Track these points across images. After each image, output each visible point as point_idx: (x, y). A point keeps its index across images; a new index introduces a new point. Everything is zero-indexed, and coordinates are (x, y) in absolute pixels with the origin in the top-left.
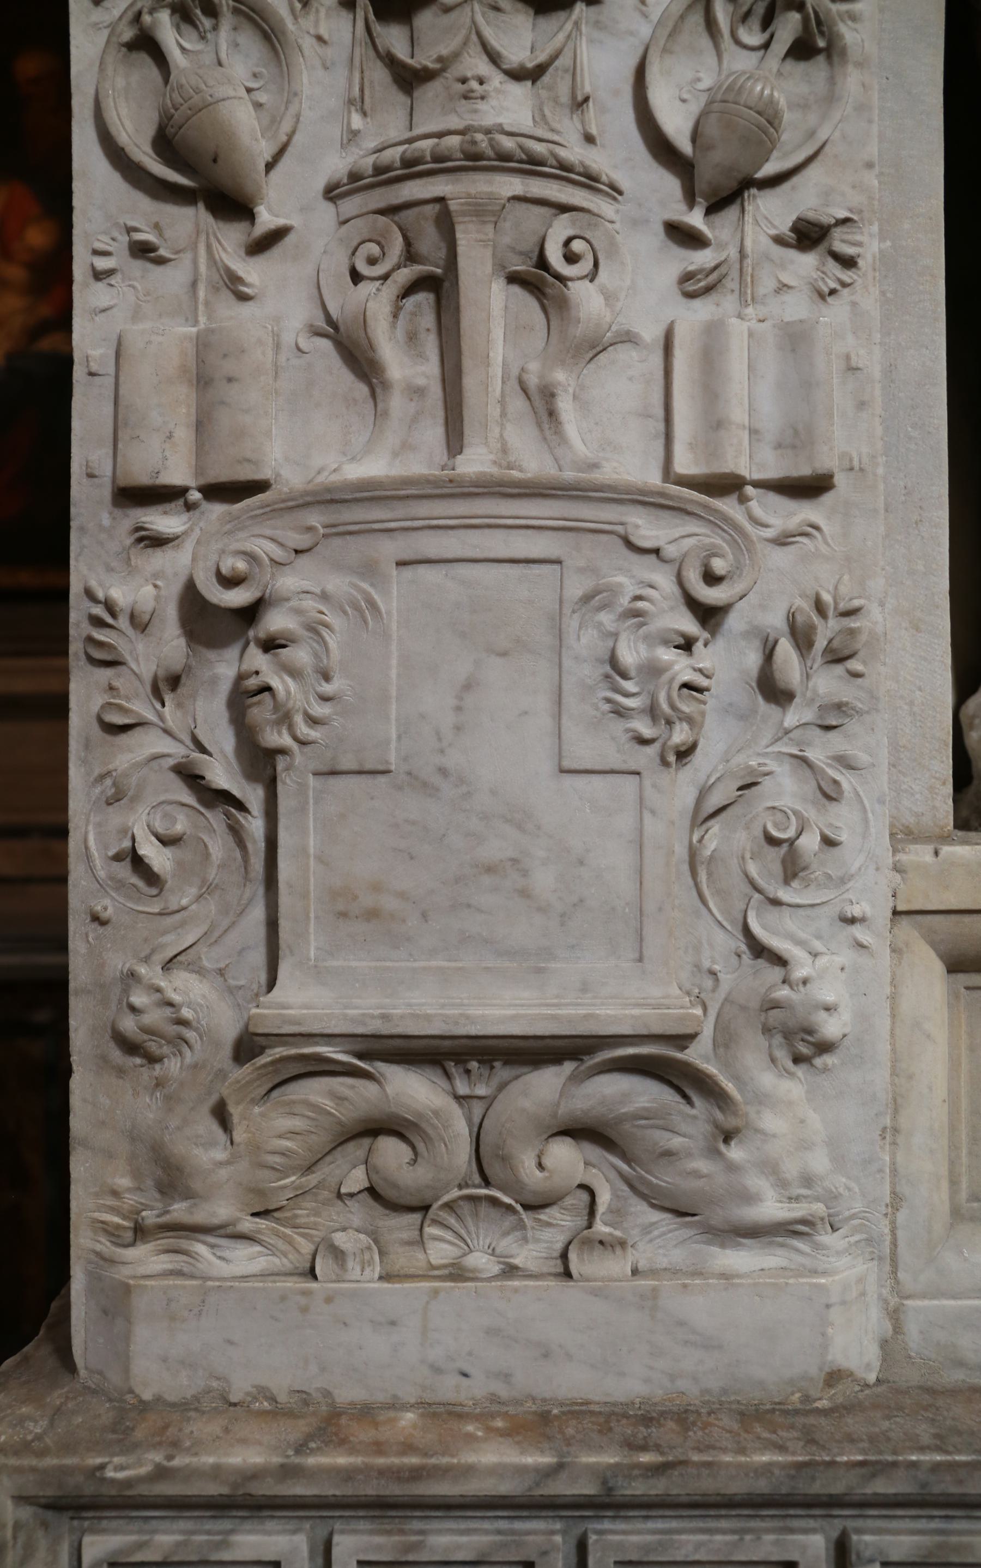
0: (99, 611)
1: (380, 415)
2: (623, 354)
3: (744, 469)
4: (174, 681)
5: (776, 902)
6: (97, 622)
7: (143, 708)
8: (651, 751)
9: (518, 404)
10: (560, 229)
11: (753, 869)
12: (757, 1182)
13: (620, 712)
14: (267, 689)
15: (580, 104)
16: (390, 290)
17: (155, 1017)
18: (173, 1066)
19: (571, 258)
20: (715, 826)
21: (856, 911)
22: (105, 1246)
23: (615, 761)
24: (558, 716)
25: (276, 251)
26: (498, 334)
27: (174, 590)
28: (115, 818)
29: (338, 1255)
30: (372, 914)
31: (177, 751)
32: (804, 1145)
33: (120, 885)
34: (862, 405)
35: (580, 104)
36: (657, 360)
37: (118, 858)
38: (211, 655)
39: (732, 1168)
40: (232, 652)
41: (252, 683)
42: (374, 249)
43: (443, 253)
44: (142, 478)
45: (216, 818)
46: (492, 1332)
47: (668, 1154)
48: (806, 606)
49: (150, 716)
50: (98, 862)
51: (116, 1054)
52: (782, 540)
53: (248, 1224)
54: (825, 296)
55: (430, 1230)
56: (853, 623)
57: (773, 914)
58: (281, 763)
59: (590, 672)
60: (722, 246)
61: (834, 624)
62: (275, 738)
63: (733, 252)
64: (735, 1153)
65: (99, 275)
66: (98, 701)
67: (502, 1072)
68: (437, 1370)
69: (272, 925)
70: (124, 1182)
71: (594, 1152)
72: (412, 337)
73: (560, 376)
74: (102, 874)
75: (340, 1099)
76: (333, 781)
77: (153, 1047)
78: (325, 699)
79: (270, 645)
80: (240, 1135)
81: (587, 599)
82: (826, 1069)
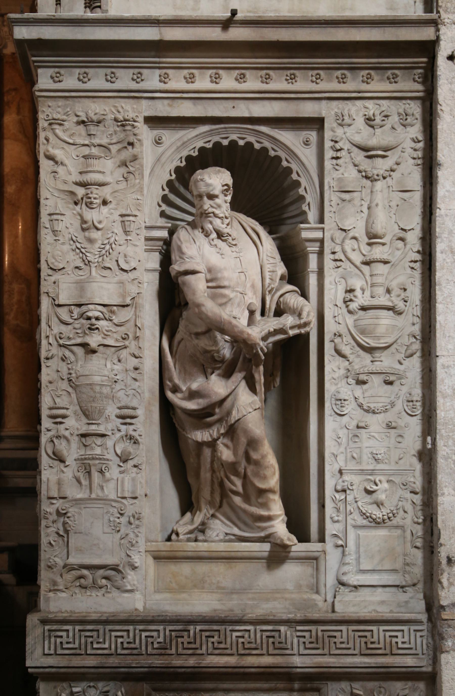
0: (45, 512)
1: (81, 489)
2: (113, 481)
3: (126, 496)
4: (55, 521)
5: (130, 550)
6: (45, 514)
7: (51, 524)
8: (114, 531)
9: (99, 487)
10: (104, 466)
11: (128, 545)
12: (127, 584)
13: (111, 526)
14: (68, 523)
15: (107, 449)
16: (83, 474)
17: (53, 563)
18: (55, 570)
19: (105, 470)
20: (123, 540)
21: (140, 551)
22: (45, 593)
23: (110, 532)
24: (103, 527)
25: (68, 467)
26: (96, 479)
27: (55, 510)
28: (48, 538)
29: (76, 593)
30: (80, 550)
31: (55, 530)
32: (133, 580)
33: (48, 547)
34: (142, 487)
35: (107, 449)
36: (116, 482)
37: (48, 543)
38: (60, 518)
39: (124, 582)
40: (63, 518)
41: (66, 522)
42: (80, 468)
43: (89, 469)
44: (51, 496)
45: (61, 538)
46: (95, 603)
47: (116, 581)
48: (134, 513)
49: (52, 525)
50: (45, 544)
51: (47, 568)
52: (132, 504)
53: (64, 590)
54: (137, 473)
55: (87, 591)
56: (140, 515)
57: (130, 551)
58: (69, 532)
59: (107, 521)
60: (125, 467)
61: (138, 515)
62: (69, 529)
63: (126, 468)
64: (124, 580)
65: (45, 469)
66: (45, 524)
67: (96, 570)
68: (88, 608)
69: (68, 552)
70: (48, 585)
71: (108, 581)
72: (85, 478)
73: (104, 484)
74: (46, 545)
75: (76, 573)
76: (76, 534)
77: (52, 567)
78: (75, 524)
79: (68, 517)
80: (64, 577)
81: (107, 512)
82: (136, 571)
